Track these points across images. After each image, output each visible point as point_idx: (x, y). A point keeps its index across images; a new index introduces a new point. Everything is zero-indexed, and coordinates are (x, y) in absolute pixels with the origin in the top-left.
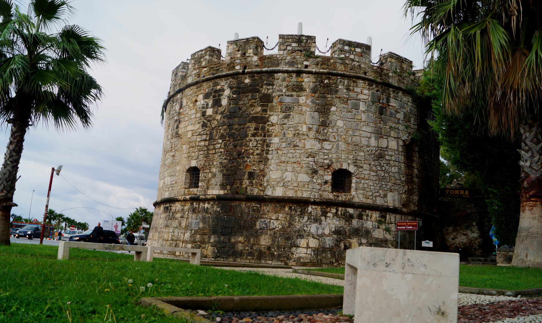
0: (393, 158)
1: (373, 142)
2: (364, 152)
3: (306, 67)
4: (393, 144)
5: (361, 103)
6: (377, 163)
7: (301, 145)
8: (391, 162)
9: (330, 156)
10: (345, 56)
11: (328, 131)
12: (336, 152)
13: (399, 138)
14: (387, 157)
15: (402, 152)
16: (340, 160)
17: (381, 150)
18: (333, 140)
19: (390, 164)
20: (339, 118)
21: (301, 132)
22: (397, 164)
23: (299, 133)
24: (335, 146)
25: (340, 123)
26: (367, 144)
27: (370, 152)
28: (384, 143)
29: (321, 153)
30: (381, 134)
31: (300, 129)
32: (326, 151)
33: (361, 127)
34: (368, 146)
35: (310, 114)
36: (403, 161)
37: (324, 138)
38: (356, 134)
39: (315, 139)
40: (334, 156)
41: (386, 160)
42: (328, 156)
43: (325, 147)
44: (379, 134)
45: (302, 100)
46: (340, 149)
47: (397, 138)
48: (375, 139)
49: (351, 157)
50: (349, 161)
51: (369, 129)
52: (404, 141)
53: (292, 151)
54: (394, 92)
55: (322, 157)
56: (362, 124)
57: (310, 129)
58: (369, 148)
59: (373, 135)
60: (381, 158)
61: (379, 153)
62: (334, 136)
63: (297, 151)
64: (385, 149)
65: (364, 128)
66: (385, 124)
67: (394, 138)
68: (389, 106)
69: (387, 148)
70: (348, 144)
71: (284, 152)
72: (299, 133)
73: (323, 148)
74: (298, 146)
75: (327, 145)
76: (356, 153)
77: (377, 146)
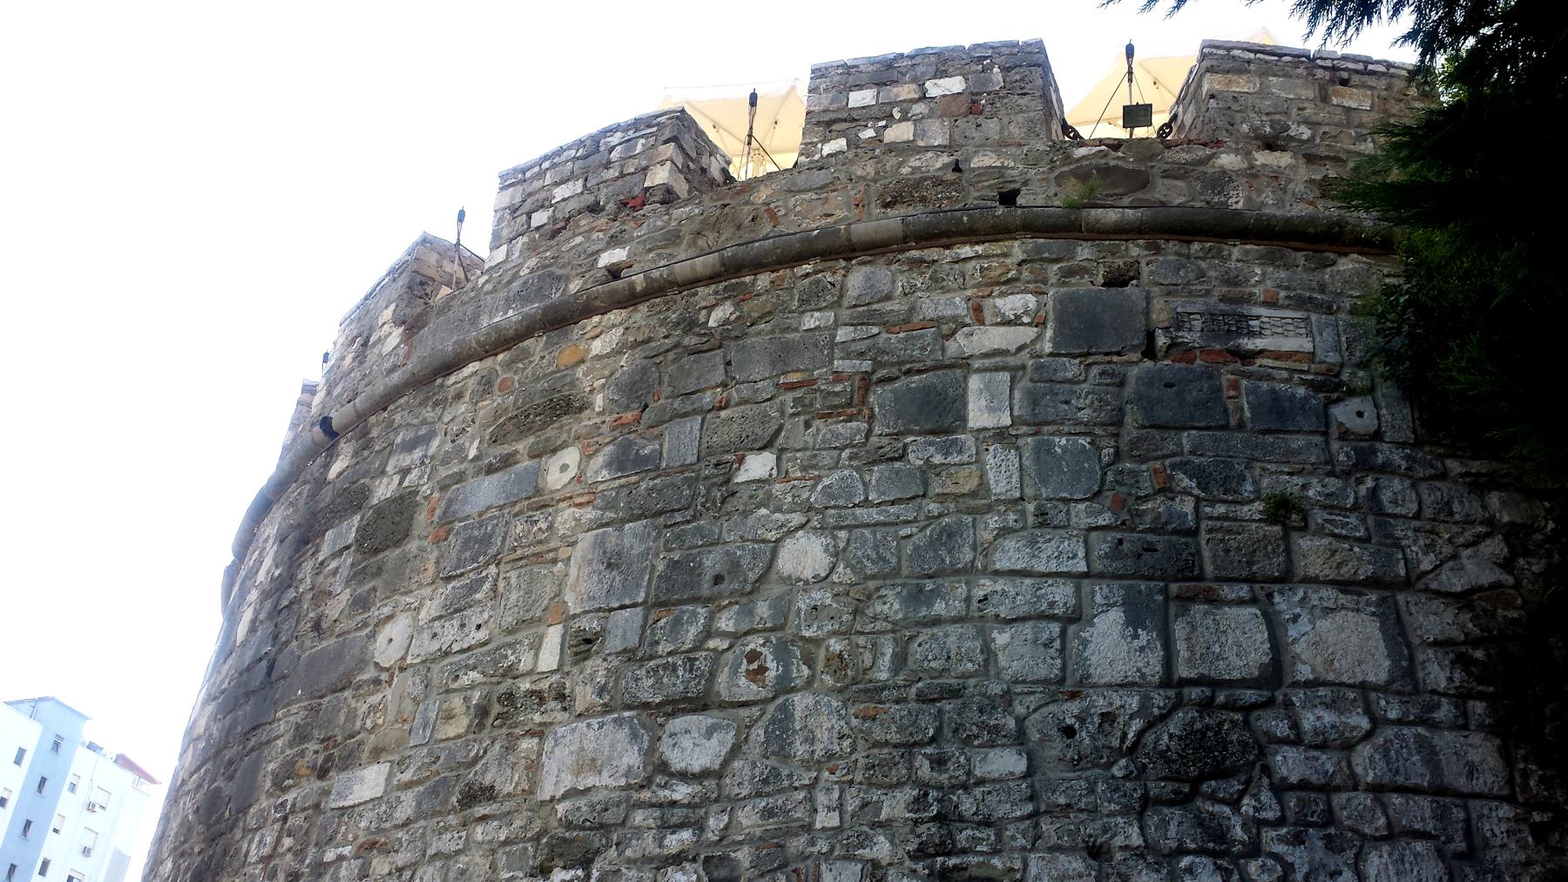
0: (1365, 762)
1: (1112, 646)
2: (1019, 739)
3: (614, 272)
4: (1338, 640)
5: (975, 382)
6: (1174, 827)
7: (507, 782)
8: (1351, 806)
9: (715, 823)
10: (853, 143)
11: (708, 633)
12: (767, 784)
13: (1407, 584)
14: (1290, 764)
15: (1461, 698)
16: (797, 844)
17: (1206, 705)
18: (747, 689)
19: (1329, 818)
20: (797, 519)
21: (525, 685)
22: (1420, 812)
23: (510, 697)
24: (758, 733)
25: (805, 555)
26: (1048, 667)
27: (1084, 738)
28: (1233, 640)
29: (639, 817)
30: (1189, 570)
31: (525, 663)
32: (682, 792)
33: (986, 551)
34: (1068, 684)
35: (600, 543)
36: (1489, 780)
37: (676, 684)
38: (939, 608)
39: (607, 709)
40: (748, 818)
41: (1281, 789)
42: (699, 826)
43: (677, 761)
44: (1165, 575)
45: (561, 470)
46: (800, 749)
47: (1373, 582)
48: (1134, 621)
49: (895, 805)
50: (882, 849)
51: (1062, 552)
52: (1463, 600)
53: (447, 843)
54: (1269, 260)
55: (649, 844)
56: (993, 521)
57: (583, 646)
58: (1074, 707)
59: (1099, 593)
60: (1223, 774)
61: (1193, 739)
62: (753, 656)
63: (479, 832)
64: (1250, 695)
65: (1011, 555)
66: (1218, 481)
67: (1344, 586)
68: (1248, 356)
69: (1275, 673)
70: (875, 692)
71: (401, 858)
72: (510, 697)
73: (663, 767)
74: (488, 793)
75: (694, 745)
76: (939, 762)
77: (1153, 665)
